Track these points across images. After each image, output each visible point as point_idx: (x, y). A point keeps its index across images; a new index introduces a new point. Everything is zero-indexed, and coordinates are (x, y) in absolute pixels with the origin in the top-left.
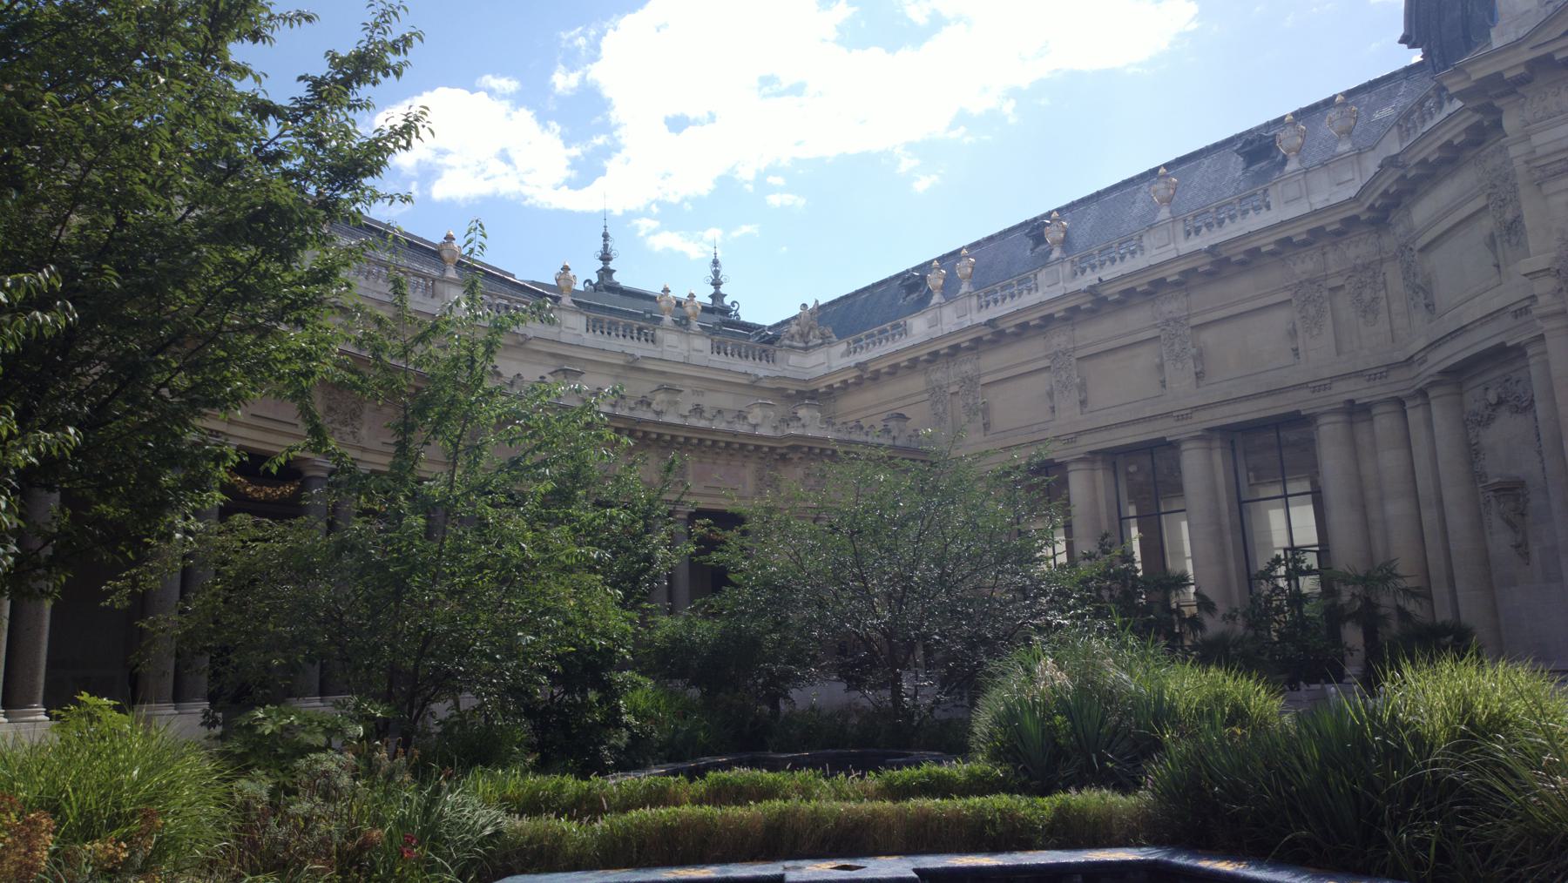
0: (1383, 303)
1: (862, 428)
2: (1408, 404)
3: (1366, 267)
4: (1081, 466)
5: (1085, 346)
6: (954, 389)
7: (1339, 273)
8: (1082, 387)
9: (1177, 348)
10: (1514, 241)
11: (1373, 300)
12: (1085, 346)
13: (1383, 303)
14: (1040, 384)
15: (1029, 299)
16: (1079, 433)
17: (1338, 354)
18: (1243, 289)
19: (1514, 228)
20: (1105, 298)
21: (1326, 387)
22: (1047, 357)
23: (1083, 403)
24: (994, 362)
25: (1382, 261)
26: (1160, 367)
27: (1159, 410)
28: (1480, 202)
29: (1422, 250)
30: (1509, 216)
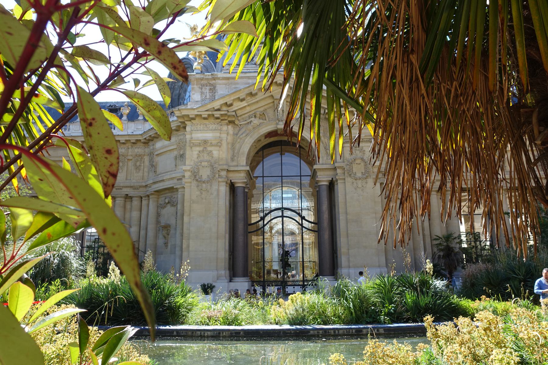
0: (142, 167)
2: (143, 199)
7: (132, 155)
10: (181, 159)
13: (142, 167)
19: (182, 156)
25: (144, 155)
28: (175, 147)
29: (156, 155)
30: (181, 153)
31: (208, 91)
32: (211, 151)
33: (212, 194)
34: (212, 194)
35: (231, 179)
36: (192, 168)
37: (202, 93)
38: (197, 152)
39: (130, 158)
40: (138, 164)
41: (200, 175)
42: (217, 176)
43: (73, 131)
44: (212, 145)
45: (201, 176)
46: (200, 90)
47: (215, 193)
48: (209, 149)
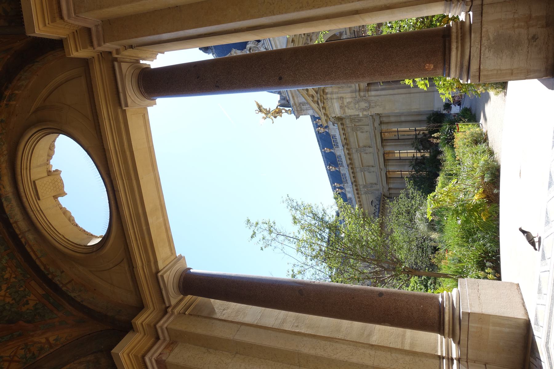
1: (375, 213)
3: (351, 121)
4: (387, 168)
5: (360, 166)
6: (366, 190)
7: (352, 125)
8: (369, 166)
9: (363, 150)
11: (358, 120)
12: (360, 166)
14: (366, 173)
15: (347, 175)
16: (380, 168)
17: (369, 125)
18: (352, 140)
20: (350, 163)
21: (375, 128)
22: (361, 172)
23: (373, 166)
24: (361, 181)
26: (366, 153)
27: (376, 154)
31: (305, 107)
32: (347, 103)
33: (378, 100)
34: (378, 100)
35: (365, 87)
36: (361, 112)
37: (307, 110)
38: (349, 111)
39: (353, 125)
40: (357, 120)
41: (365, 107)
42: (364, 98)
43: (341, 153)
44: (343, 103)
45: (366, 107)
46: (305, 111)
47: (377, 98)
48: (346, 104)
